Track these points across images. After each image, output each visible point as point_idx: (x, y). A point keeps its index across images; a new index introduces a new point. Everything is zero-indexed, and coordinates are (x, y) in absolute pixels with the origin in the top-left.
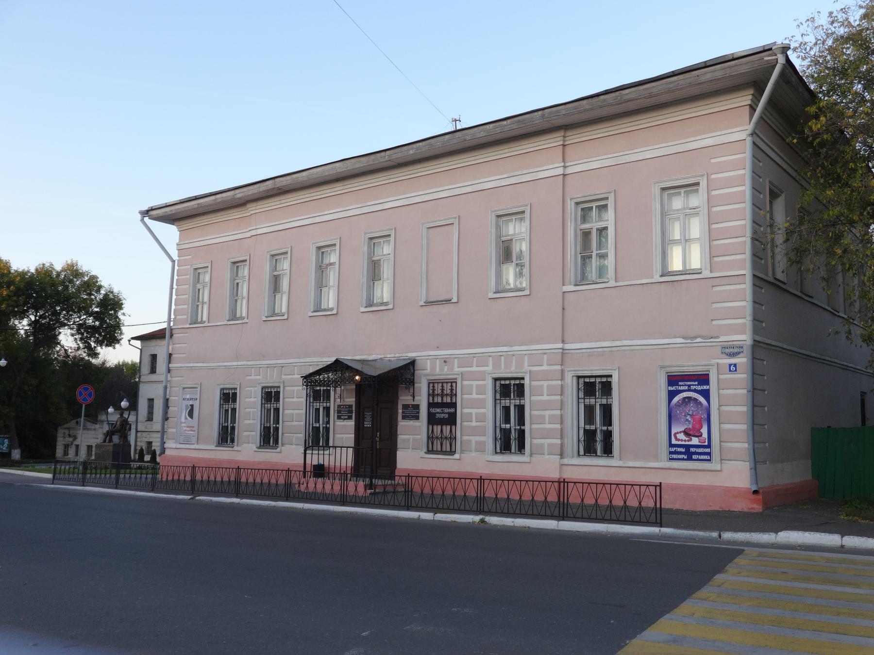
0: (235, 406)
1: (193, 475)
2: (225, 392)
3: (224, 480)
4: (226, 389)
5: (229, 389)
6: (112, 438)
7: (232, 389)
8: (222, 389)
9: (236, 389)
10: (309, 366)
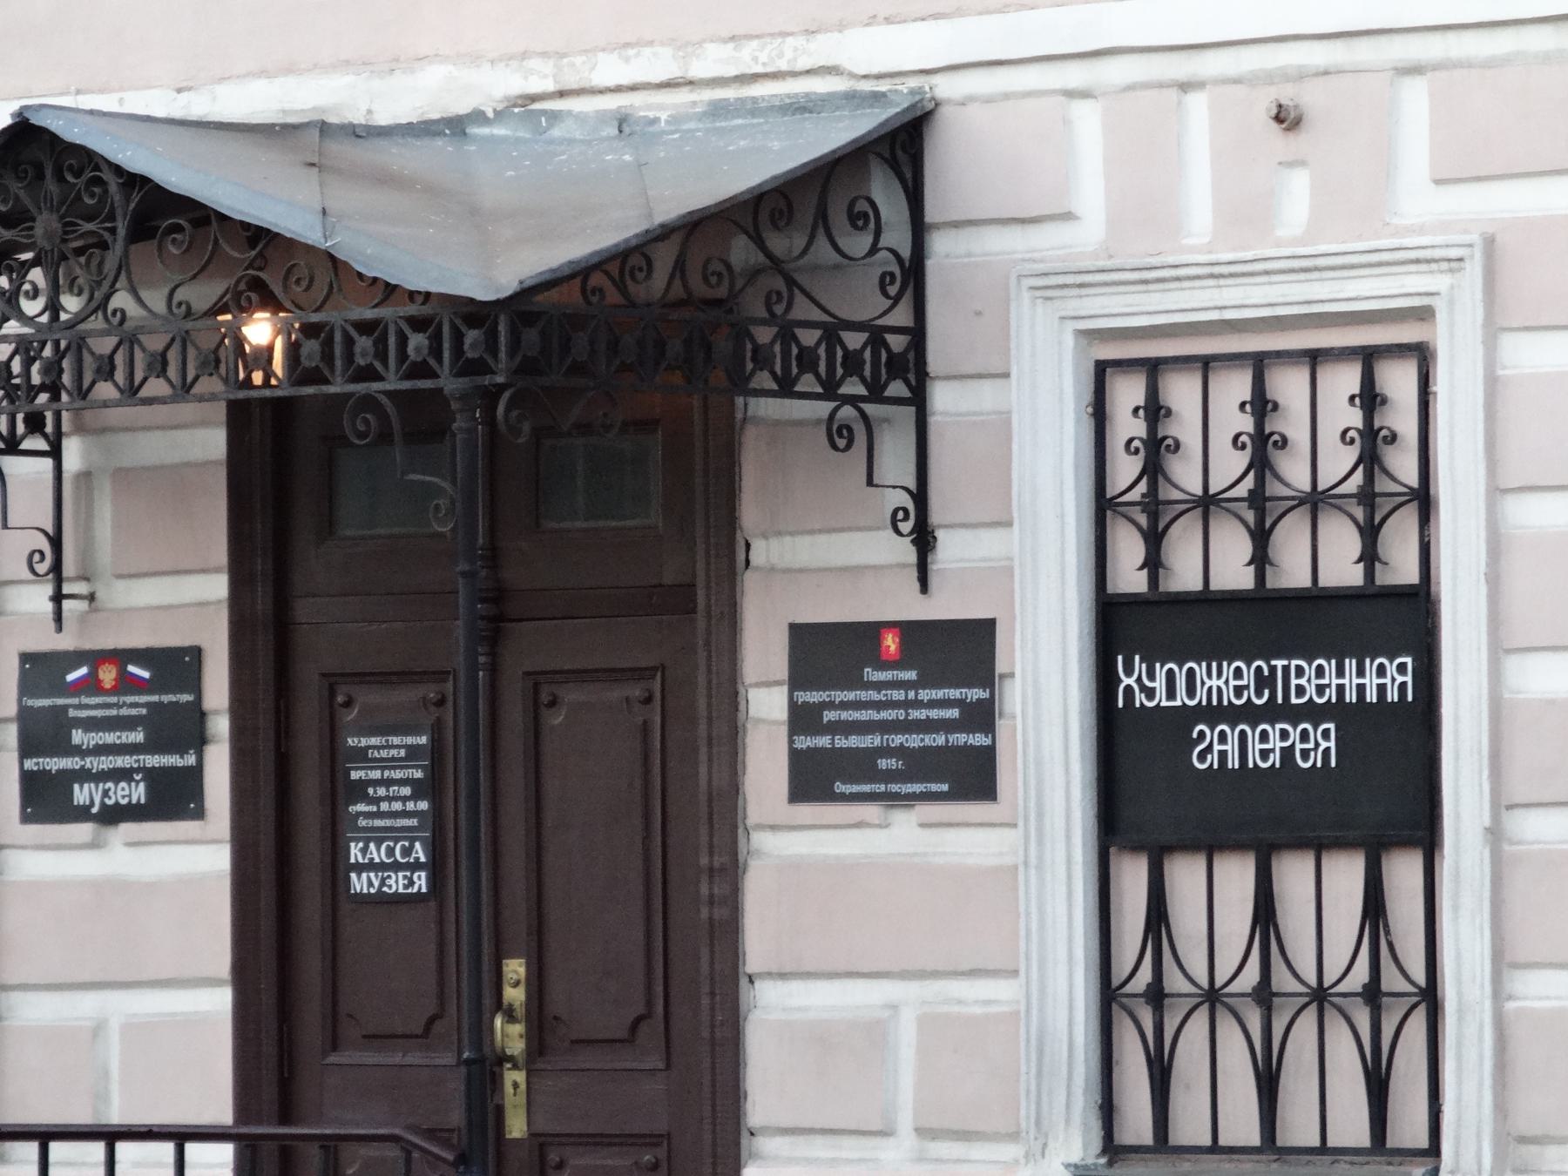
6: (1224, 1147)
10: (1173, 94)
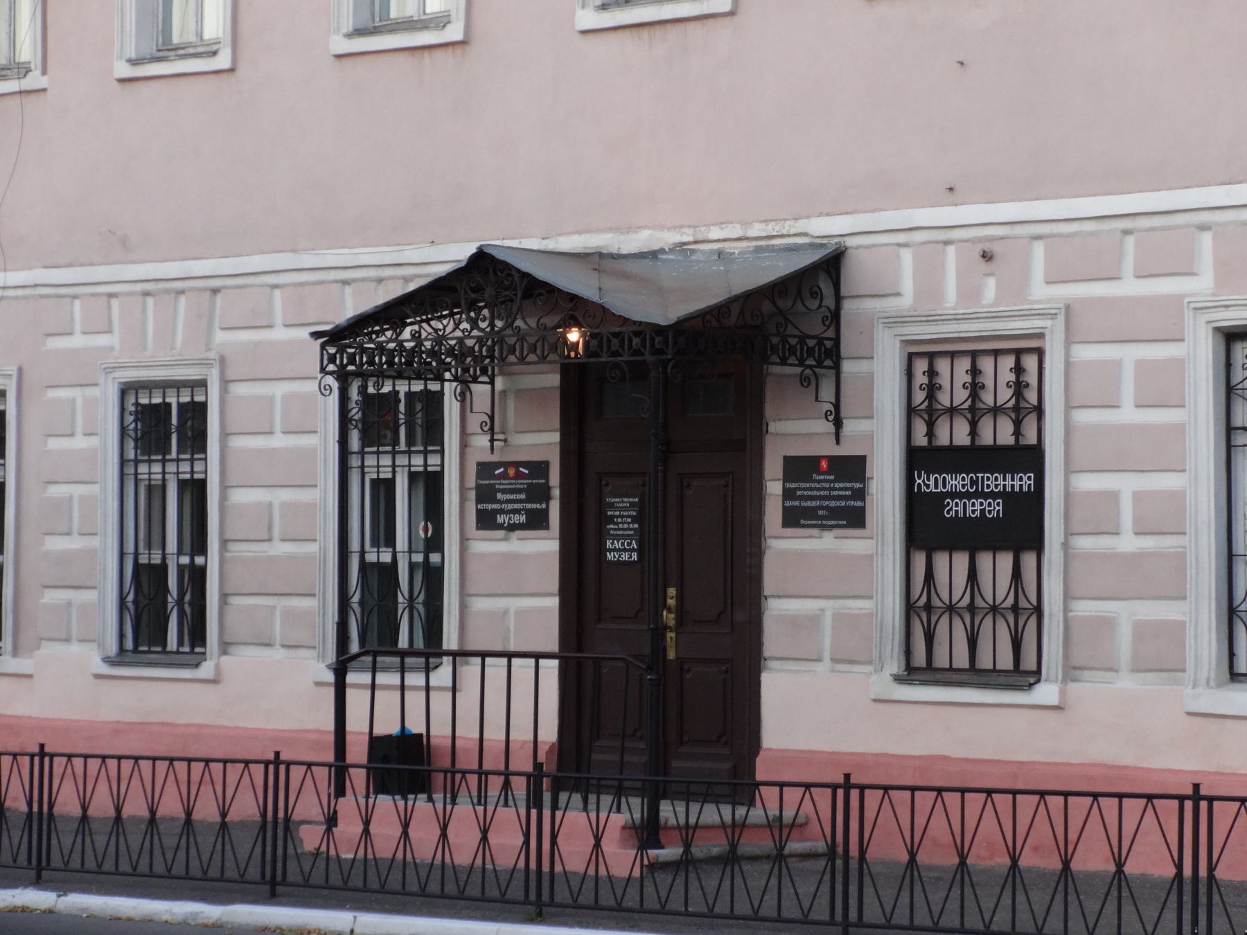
0: (198, 467)
1: (41, 787)
2: (144, 401)
3: (196, 816)
4: (149, 386)
5: (165, 385)
7: (178, 385)
8: (125, 390)
9: (203, 384)
10: (941, 246)
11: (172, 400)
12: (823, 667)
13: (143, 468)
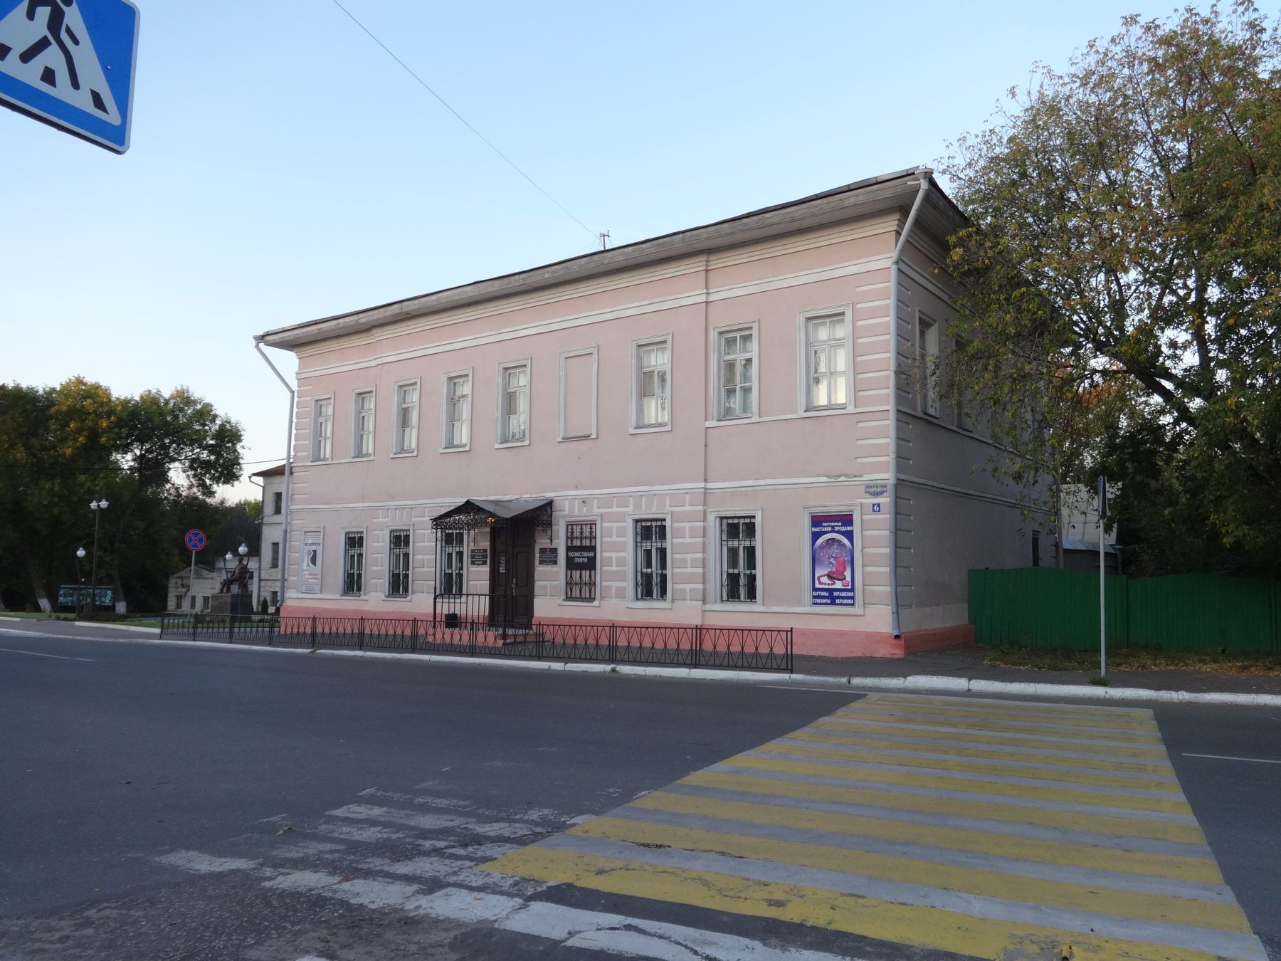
2: (350, 536)
4: (352, 533)
5: (355, 533)
8: (347, 533)
9: (363, 532)
11: (356, 536)
12: (210, 596)
13: (350, 551)
